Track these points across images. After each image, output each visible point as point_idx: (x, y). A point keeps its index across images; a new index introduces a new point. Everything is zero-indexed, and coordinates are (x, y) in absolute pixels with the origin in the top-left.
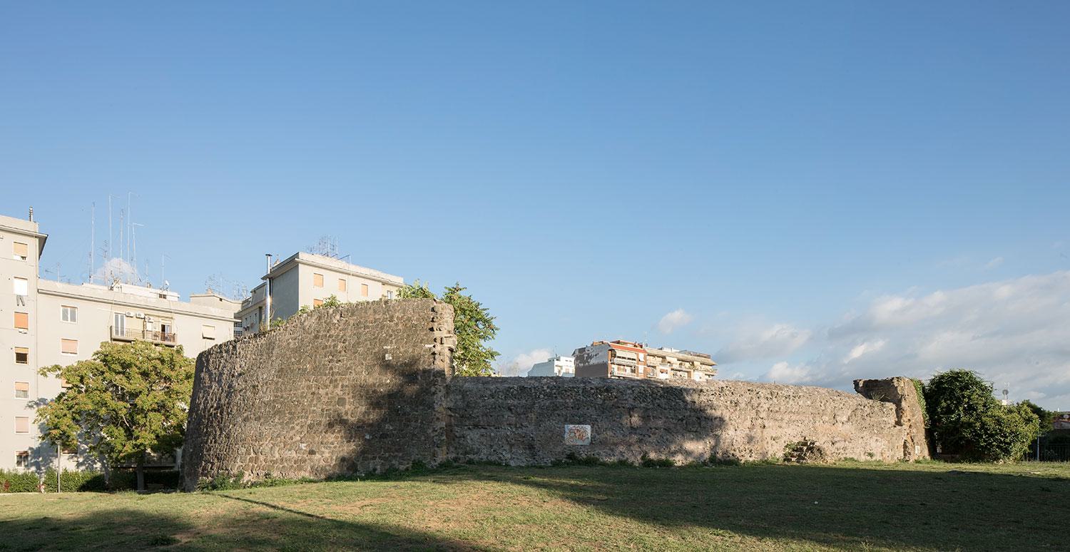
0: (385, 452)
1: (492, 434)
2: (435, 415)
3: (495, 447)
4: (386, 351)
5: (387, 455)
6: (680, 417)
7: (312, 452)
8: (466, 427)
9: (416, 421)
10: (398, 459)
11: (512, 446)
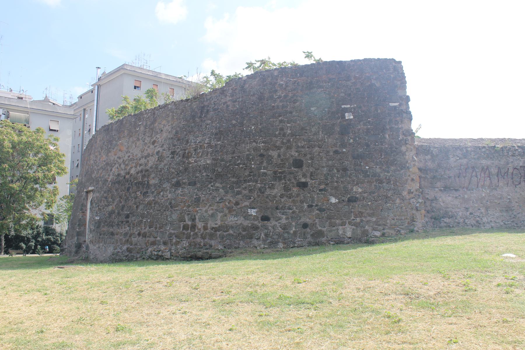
0: (356, 216)
1: (466, 196)
2: (409, 176)
3: (470, 210)
5: (358, 220)
7: (265, 218)
8: (437, 189)
9: (389, 183)
10: (371, 224)
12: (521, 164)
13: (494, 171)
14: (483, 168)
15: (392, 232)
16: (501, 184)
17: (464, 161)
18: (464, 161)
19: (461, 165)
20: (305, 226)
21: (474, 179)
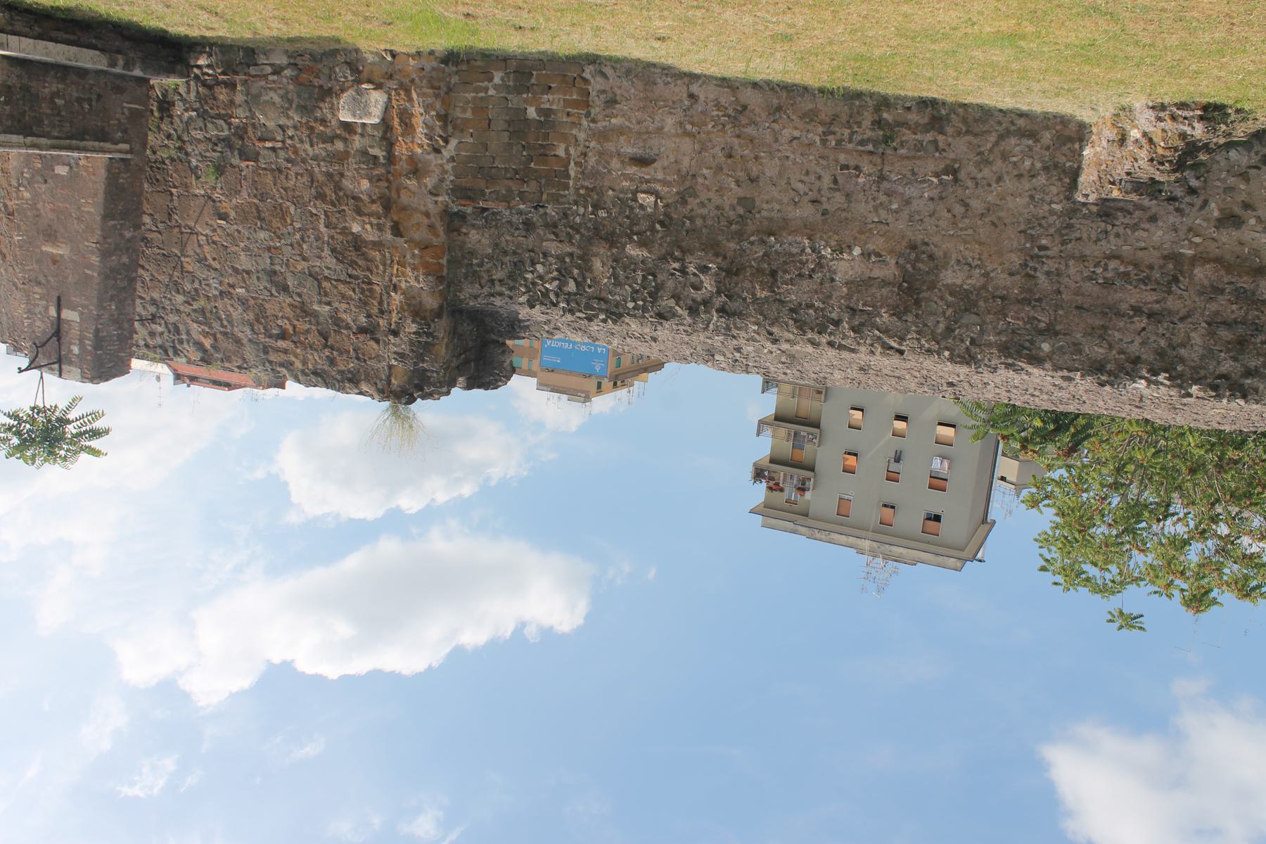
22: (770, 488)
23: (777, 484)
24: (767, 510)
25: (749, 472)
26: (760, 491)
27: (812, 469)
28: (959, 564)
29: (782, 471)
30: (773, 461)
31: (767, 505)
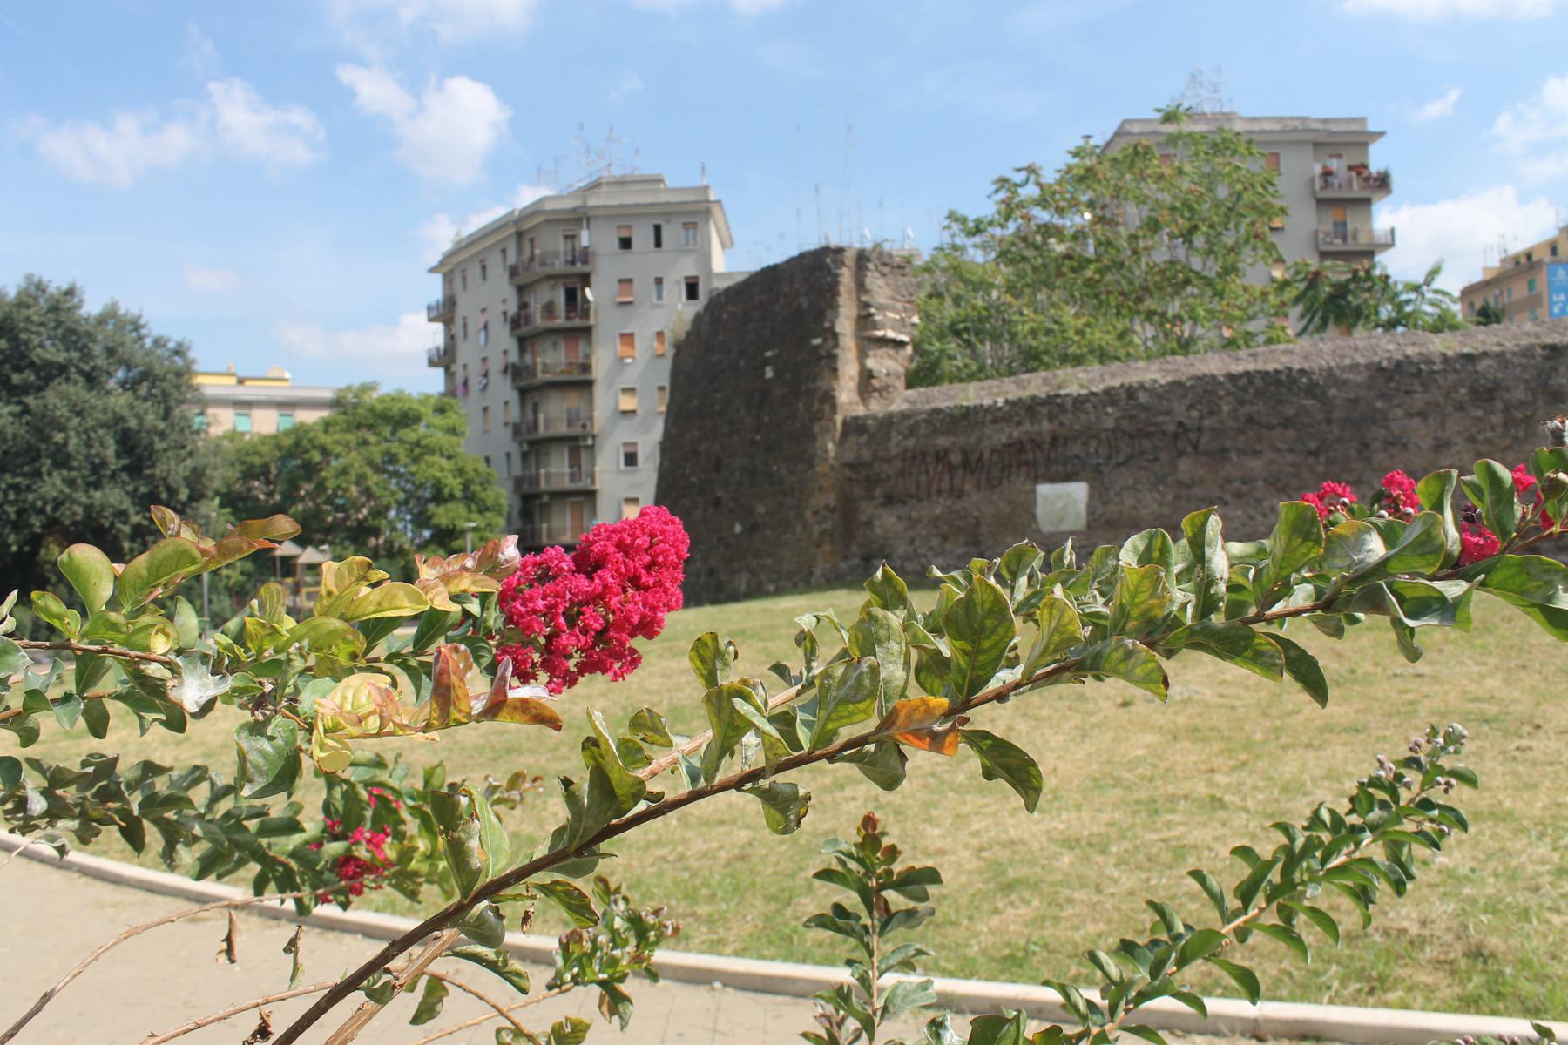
1: (914, 514)
3: (918, 542)
4: (767, 362)
6: (1313, 445)
11: (945, 538)
12: (1004, 440)
13: (955, 458)
14: (937, 454)
15: (789, 584)
16: (968, 486)
17: (911, 442)
18: (911, 442)
19: (905, 451)
20: (711, 572)
21: (923, 478)
22: (1365, 166)
23: (1359, 174)
24: (1359, 139)
25: (1396, 182)
26: (1377, 160)
27: (1321, 202)
28: (1127, 127)
29: (1356, 190)
30: (1366, 202)
31: (1364, 145)
